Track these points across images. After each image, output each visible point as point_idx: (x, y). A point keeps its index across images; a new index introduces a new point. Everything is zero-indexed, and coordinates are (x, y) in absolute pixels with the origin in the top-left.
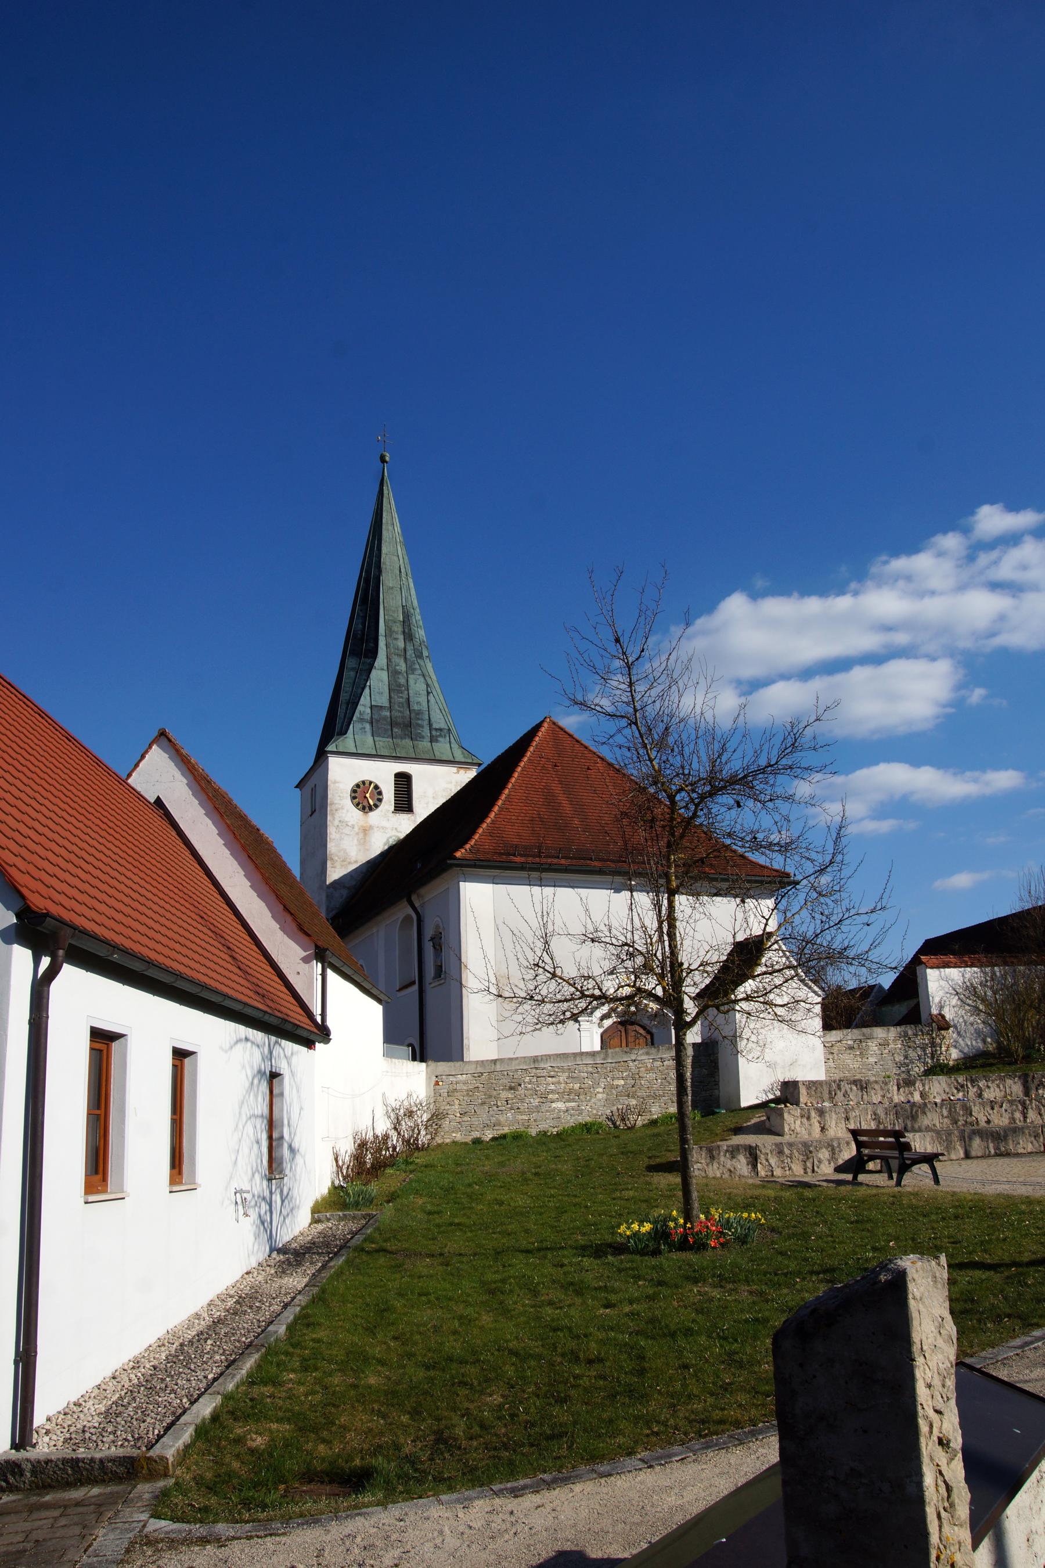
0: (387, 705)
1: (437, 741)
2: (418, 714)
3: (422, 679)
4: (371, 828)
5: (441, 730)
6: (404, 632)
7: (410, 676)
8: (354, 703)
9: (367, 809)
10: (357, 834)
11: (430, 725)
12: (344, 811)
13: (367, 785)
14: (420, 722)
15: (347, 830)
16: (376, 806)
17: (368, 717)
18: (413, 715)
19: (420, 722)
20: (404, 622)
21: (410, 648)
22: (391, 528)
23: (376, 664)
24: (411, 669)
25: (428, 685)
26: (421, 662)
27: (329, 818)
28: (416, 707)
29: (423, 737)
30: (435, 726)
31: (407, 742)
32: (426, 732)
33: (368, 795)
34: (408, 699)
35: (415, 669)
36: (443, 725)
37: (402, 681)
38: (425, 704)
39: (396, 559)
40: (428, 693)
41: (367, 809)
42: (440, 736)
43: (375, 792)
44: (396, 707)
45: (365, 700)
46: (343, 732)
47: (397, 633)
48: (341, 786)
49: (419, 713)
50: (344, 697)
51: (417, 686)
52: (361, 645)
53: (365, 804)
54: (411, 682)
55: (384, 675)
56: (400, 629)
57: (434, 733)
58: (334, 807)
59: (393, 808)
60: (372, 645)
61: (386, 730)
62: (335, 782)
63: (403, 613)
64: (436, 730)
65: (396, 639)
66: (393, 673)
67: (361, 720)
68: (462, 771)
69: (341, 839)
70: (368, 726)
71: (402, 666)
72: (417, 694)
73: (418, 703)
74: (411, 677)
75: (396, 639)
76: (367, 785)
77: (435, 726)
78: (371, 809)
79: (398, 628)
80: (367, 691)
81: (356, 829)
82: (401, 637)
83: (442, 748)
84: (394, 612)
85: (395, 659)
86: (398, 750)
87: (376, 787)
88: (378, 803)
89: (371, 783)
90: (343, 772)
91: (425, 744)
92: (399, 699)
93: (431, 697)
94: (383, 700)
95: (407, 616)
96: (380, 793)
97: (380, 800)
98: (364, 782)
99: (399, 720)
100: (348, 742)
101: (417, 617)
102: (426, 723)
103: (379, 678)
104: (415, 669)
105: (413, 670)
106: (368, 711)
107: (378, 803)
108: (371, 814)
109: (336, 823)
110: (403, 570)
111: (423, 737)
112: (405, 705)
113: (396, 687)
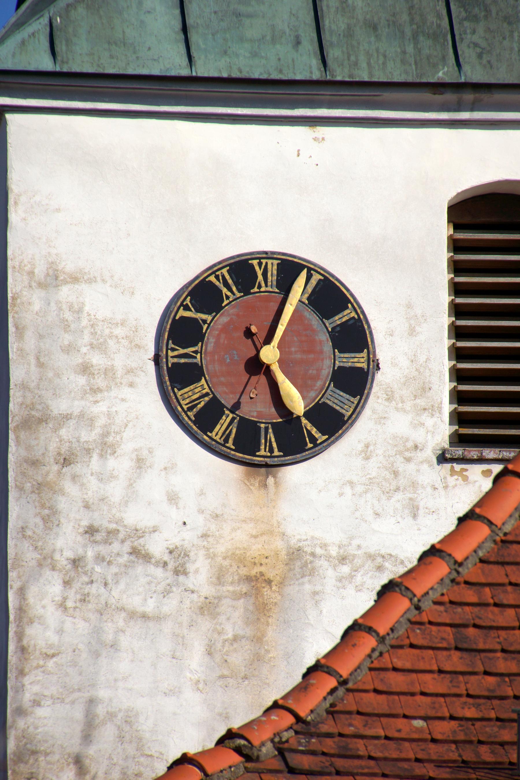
9: (269, 443)
10: (208, 608)
12: (120, 465)
13: (267, 285)
15: (137, 590)
16: (331, 423)
27: (16, 510)
33: (270, 354)
41: (269, 443)
43: (321, 331)
48: (96, 301)
53: (258, 408)
58: (50, 442)
62: (54, 278)
69: (102, 647)
76: (267, 285)
81: (200, 576)
86: (472, 35)
87: (330, 296)
88: (339, 401)
89: (289, 269)
96: (355, 336)
97: (356, 382)
98: (242, 270)
107: (339, 401)
108: (296, 475)
109: (66, 541)
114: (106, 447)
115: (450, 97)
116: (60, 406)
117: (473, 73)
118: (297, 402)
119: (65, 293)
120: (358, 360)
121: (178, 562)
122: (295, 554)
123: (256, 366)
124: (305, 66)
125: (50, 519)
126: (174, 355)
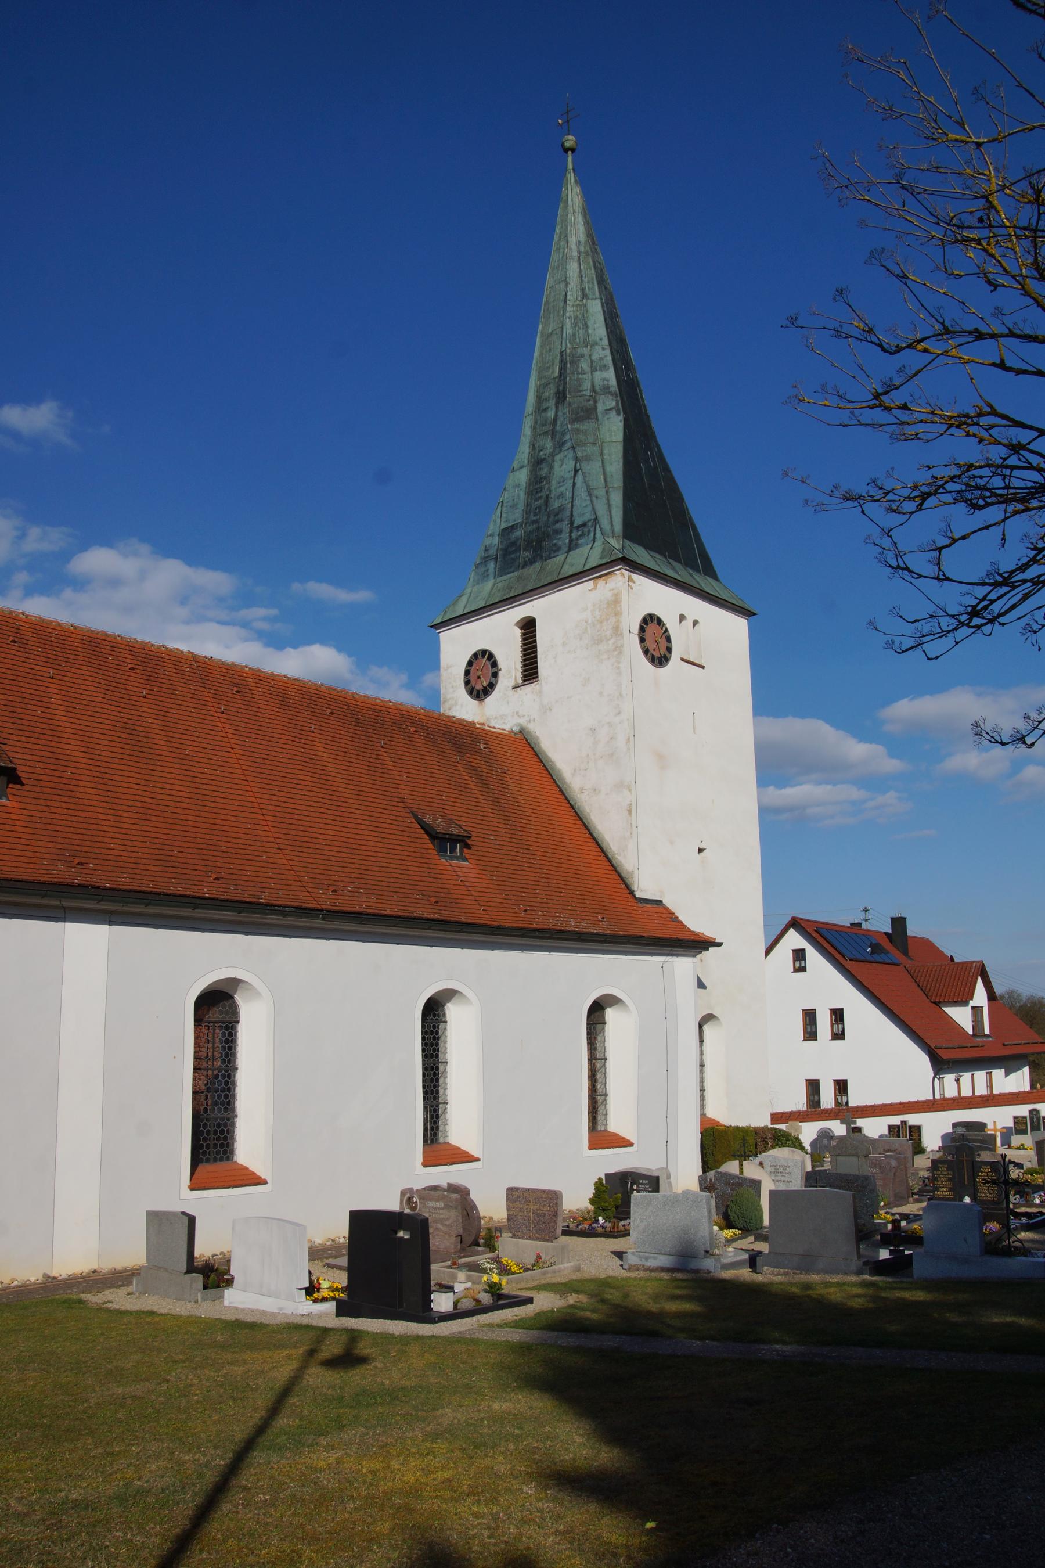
1: (577, 546)
2: (557, 514)
3: (571, 454)
5: (584, 525)
6: (557, 393)
11: (572, 523)
19: (558, 526)
20: (560, 375)
22: (563, 243)
24: (560, 445)
25: (577, 459)
26: (587, 426)
28: (556, 505)
30: (578, 522)
31: (537, 566)
32: (565, 538)
34: (547, 496)
36: (588, 516)
37: (544, 472)
38: (569, 494)
39: (562, 285)
40: (576, 471)
47: (547, 400)
49: (561, 509)
51: (562, 467)
54: (557, 465)
55: (522, 476)
61: (514, 560)
62: (448, 667)
63: (561, 361)
64: (578, 527)
65: (546, 410)
66: (537, 462)
68: (601, 582)
70: (491, 565)
71: (549, 444)
72: (563, 480)
73: (561, 495)
77: (578, 522)
79: (550, 392)
82: (552, 403)
83: (576, 560)
84: (548, 368)
88: (493, 680)
91: (562, 557)
93: (579, 479)
94: (517, 516)
96: (495, 664)
97: (495, 675)
102: (564, 525)
106: (496, 540)
107: (493, 680)
108: (488, 700)
111: (559, 549)
112: (543, 508)
113: (537, 483)
114: (456, 704)
116: (449, 697)
119: (449, 671)
124: (482, 604)
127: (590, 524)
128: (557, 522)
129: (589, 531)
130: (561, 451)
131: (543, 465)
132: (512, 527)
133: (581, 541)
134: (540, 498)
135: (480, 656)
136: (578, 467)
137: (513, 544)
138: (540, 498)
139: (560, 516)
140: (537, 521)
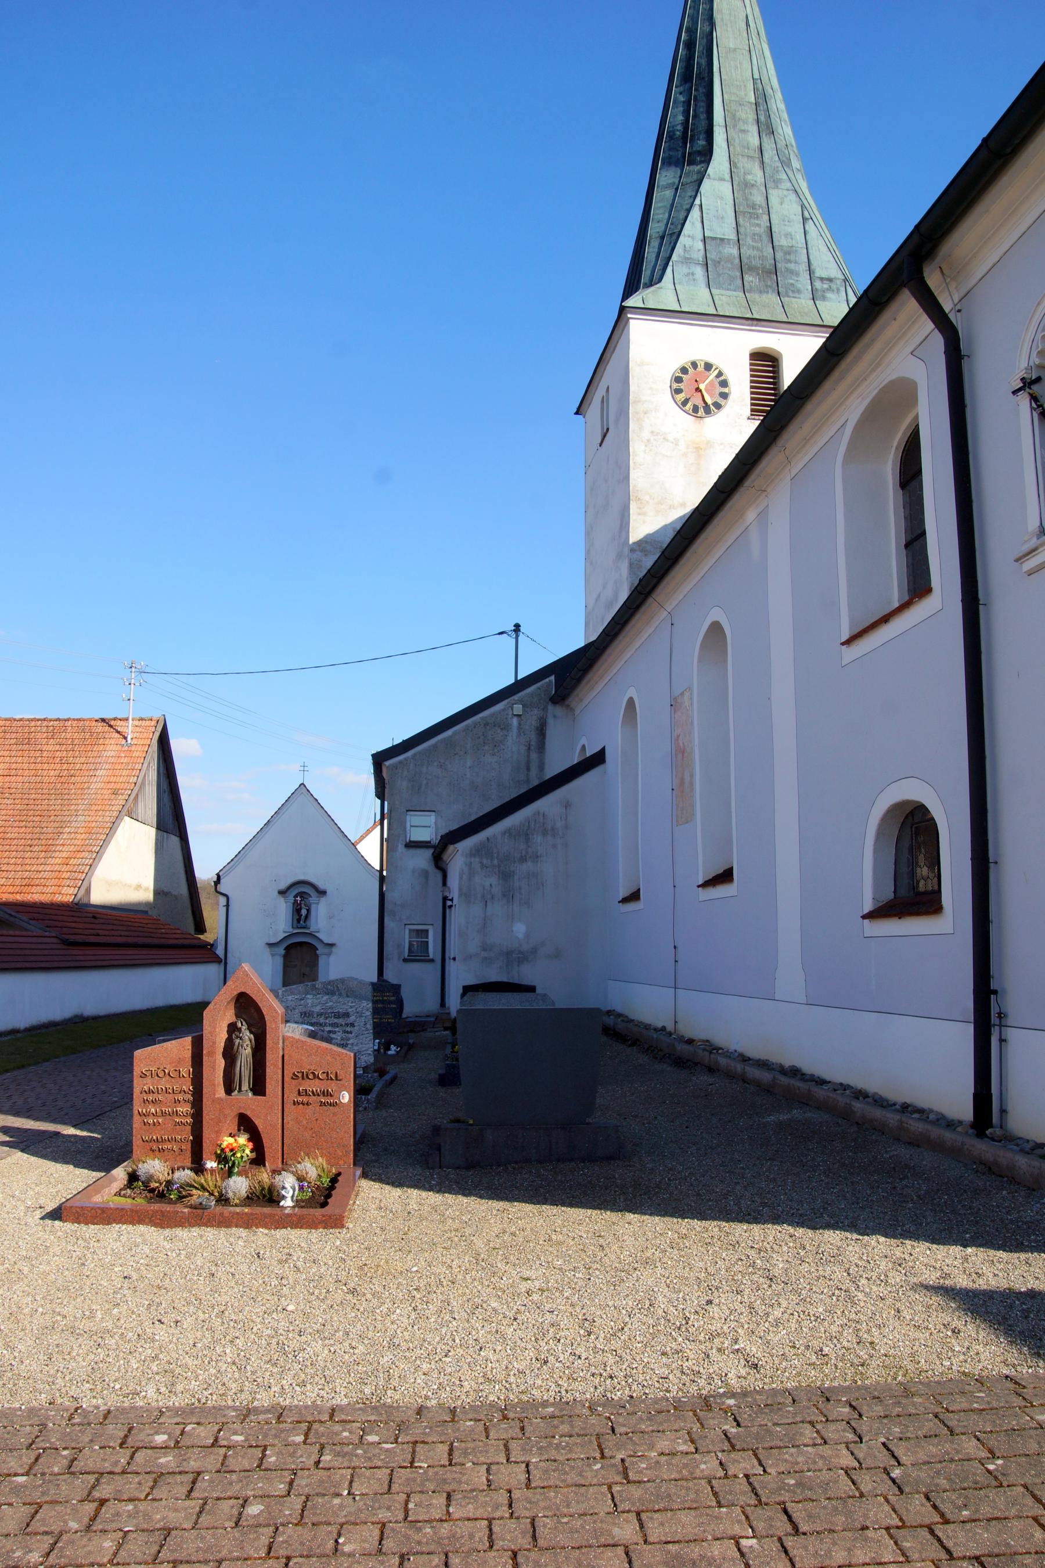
0: (733, 236)
1: (824, 298)
3: (792, 196)
4: (709, 444)
5: (830, 280)
7: (770, 191)
8: (672, 236)
10: (685, 455)
11: (811, 272)
14: (792, 266)
16: (718, 406)
17: (700, 256)
18: (779, 255)
21: (768, 145)
23: (710, 170)
29: (799, 291)
33: (702, 387)
35: (780, 181)
37: (758, 199)
42: (830, 289)
44: (749, 241)
45: (692, 229)
46: (655, 280)
47: (745, 122)
49: (790, 251)
50: (655, 228)
52: (685, 144)
54: (774, 201)
55: (726, 189)
56: (751, 116)
57: (818, 284)
59: (748, 413)
60: (702, 143)
61: (732, 279)
64: (822, 279)
67: (687, 260)
70: (699, 272)
72: (786, 220)
73: (788, 235)
74: (774, 195)
75: (744, 131)
77: (819, 273)
78: (707, 410)
79: (748, 114)
80: (695, 213)
85: (743, 163)
89: (708, 367)
90: (655, 349)
92: (754, 228)
95: (762, 99)
96: (724, 384)
97: (725, 396)
99: (757, 263)
100: (661, 295)
101: (778, 103)
102: (803, 268)
103: (716, 191)
104: (780, 181)
105: (777, 183)
109: (646, 434)
110: (750, 18)
112: (766, 238)
115: (750, 322)
117: (756, 316)
118: (709, 400)
120: (726, 390)
121: (676, 443)
122: (708, 442)
123: (698, 390)
125: (641, 428)
126: (675, 386)
127: (838, 282)
128: (790, 261)
129: (838, 290)
130: (777, 187)
131: (755, 191)
132: (722, 240)
133: (829, 295)
134: (759, 225)
135: (691, 370)
136: (806, 215)
137: (729, 259)
138: (759, 225)
139: (792, 257)
140: (758, 249)
